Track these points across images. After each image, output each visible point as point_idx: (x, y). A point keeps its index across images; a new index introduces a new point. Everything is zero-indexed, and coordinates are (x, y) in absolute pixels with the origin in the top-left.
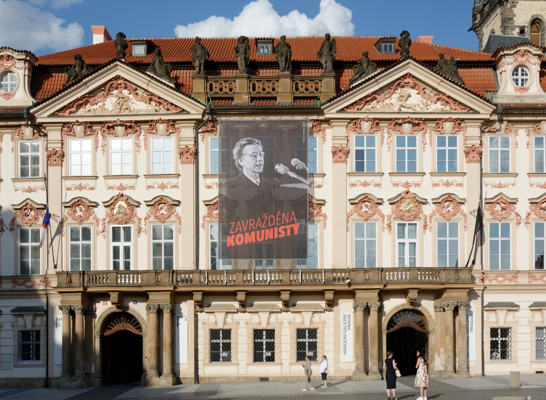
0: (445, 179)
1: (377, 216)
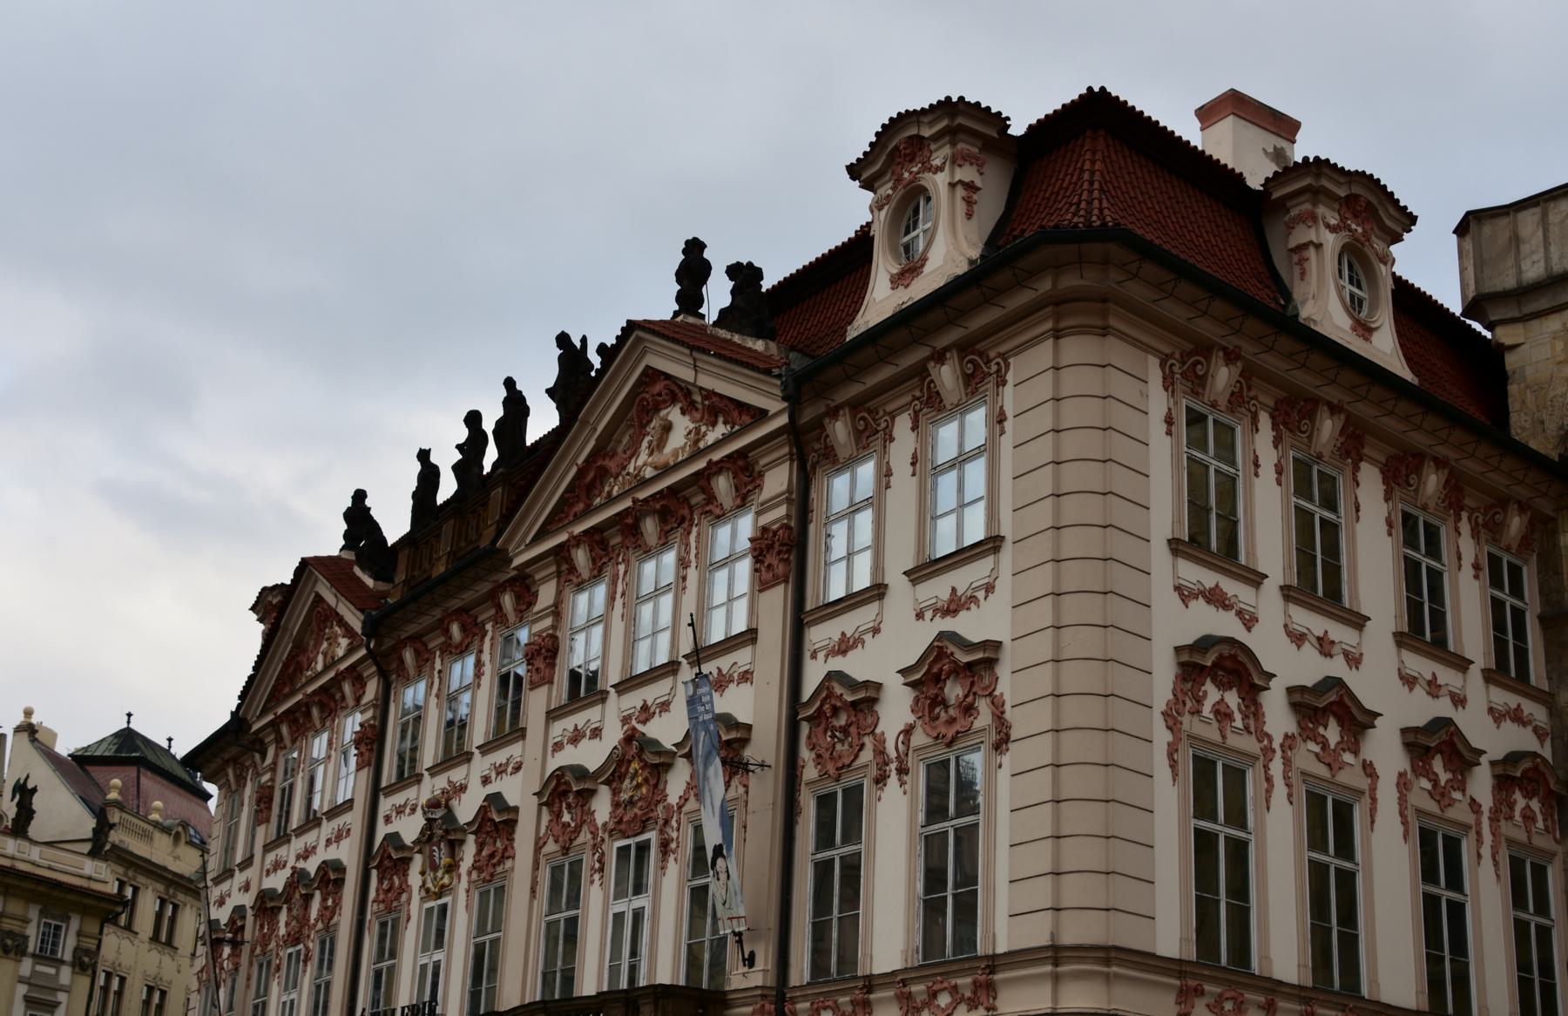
1: (585, 837)
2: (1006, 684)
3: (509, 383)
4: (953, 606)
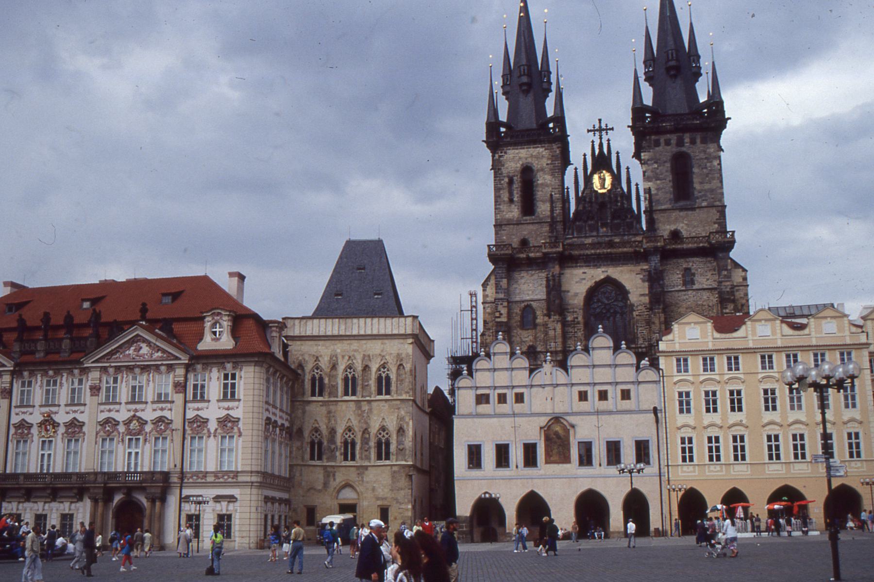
0: (160, 405)
1: (115, 433)
2: (241, 425)
3: (68, 312)
4: (228, 409)
